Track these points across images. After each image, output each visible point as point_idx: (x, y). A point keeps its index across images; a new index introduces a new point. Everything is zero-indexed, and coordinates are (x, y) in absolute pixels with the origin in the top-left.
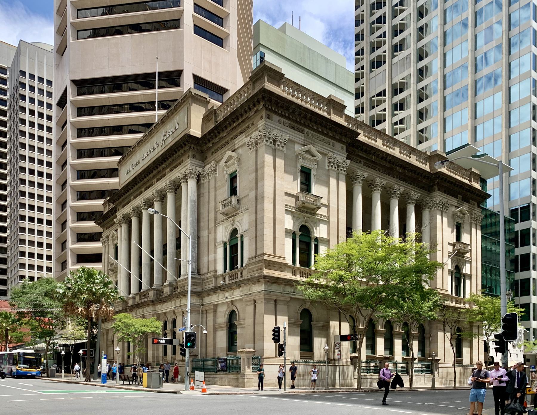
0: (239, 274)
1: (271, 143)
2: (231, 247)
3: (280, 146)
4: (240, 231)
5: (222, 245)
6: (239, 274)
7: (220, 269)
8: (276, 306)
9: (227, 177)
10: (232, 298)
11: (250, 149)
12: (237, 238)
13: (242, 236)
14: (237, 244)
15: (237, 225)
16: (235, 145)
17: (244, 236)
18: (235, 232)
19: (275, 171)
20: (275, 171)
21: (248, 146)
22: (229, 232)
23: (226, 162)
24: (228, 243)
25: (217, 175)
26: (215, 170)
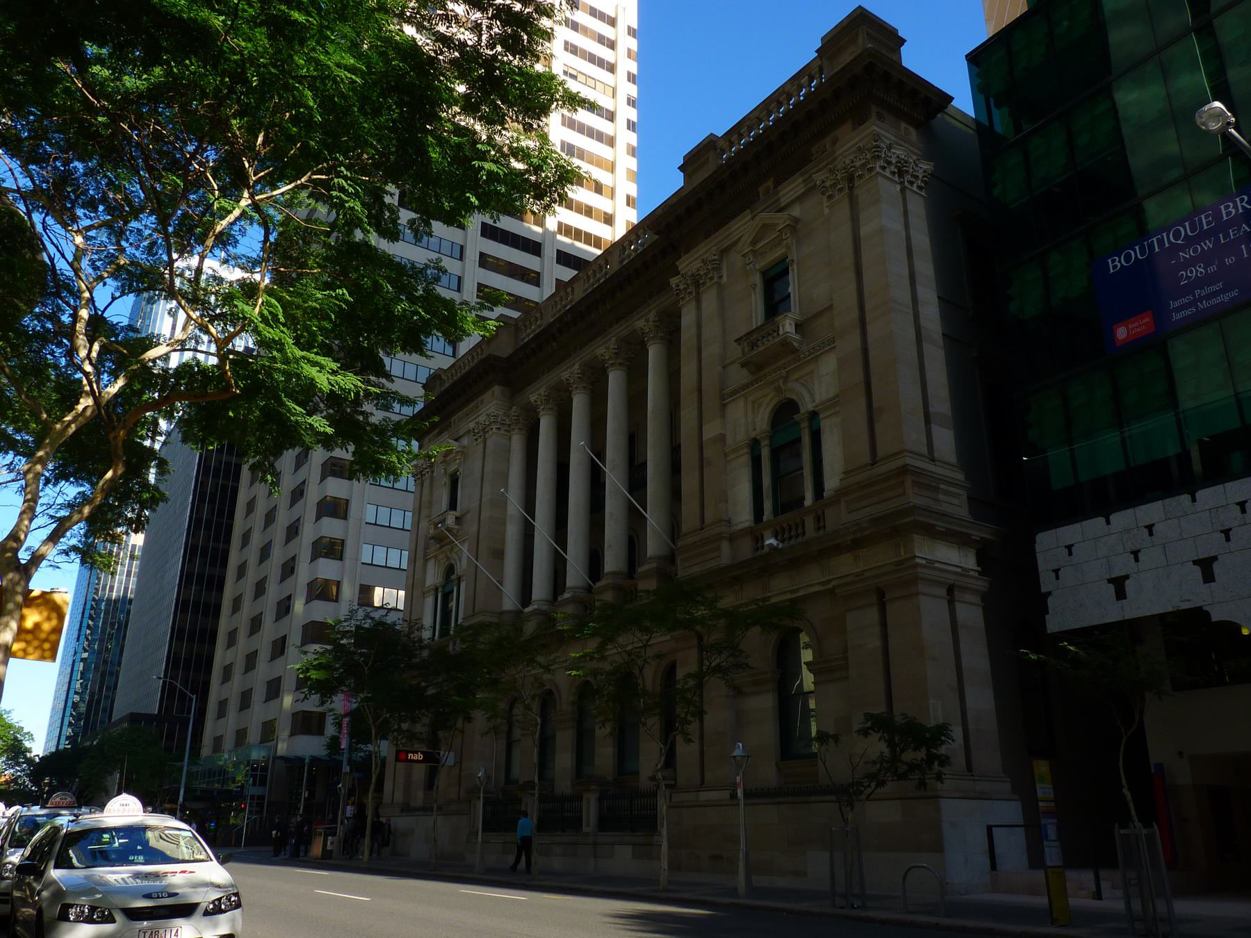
0: (810, 522)
1: (893, 173)
2: (775, 453)
3: (915, 185)
4: (807, 406)
5: (746, 450)
6: (810, 522)
7: (743, 516)
8: (951, 603)
9: (758, 279)
10: (792, 592)
11: (830, 197)
12: (797, 423)
13: (814, 415)
14: (799, 440)
15: (796, 390)
16: (779, 199)
17: (822, 416)
18: (785, 411)
19: (908, 239)
20: (908, 239)
21: (823, 193)
22: (768, 411)
23: (754, 243)
24: (765, 443)
25: (725, 279)
26: (718, 269)
